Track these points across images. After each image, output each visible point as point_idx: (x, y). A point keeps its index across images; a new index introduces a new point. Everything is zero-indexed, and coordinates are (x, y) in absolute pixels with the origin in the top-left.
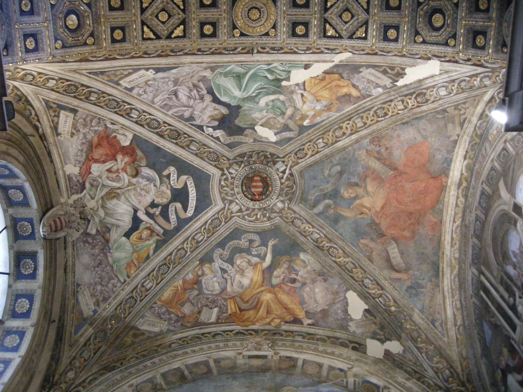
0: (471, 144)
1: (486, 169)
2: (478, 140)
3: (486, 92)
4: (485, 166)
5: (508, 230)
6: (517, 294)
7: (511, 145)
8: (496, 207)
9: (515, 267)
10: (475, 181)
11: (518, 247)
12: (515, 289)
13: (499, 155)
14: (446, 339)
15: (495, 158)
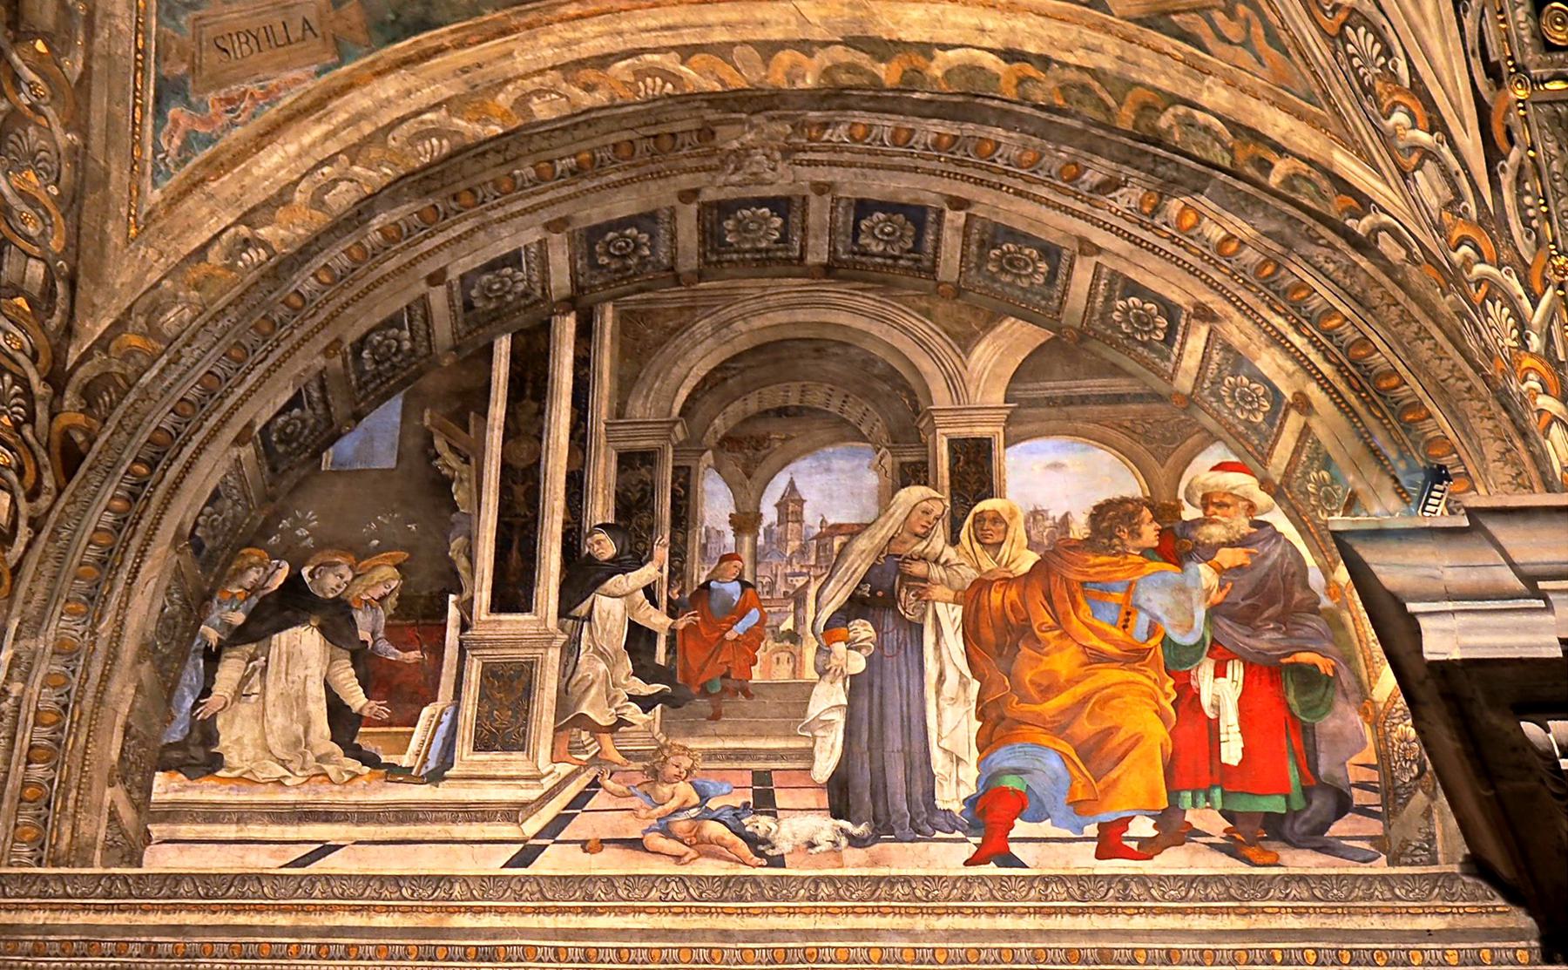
0: (1087, 78)
1: (1028, 208)
2: (1126, 118)
3: (1377, 169)
4: (1036, 199)
5: (863, 439)
6: (647, 573)
7: (1206, 358)
8: (905, 330)
9: (745, 522)
10: (937, 145)
11: (831, 521)
12: (662, 553)
13: (1132, 288)
14: (155, 196)
15: (1108, 263)
